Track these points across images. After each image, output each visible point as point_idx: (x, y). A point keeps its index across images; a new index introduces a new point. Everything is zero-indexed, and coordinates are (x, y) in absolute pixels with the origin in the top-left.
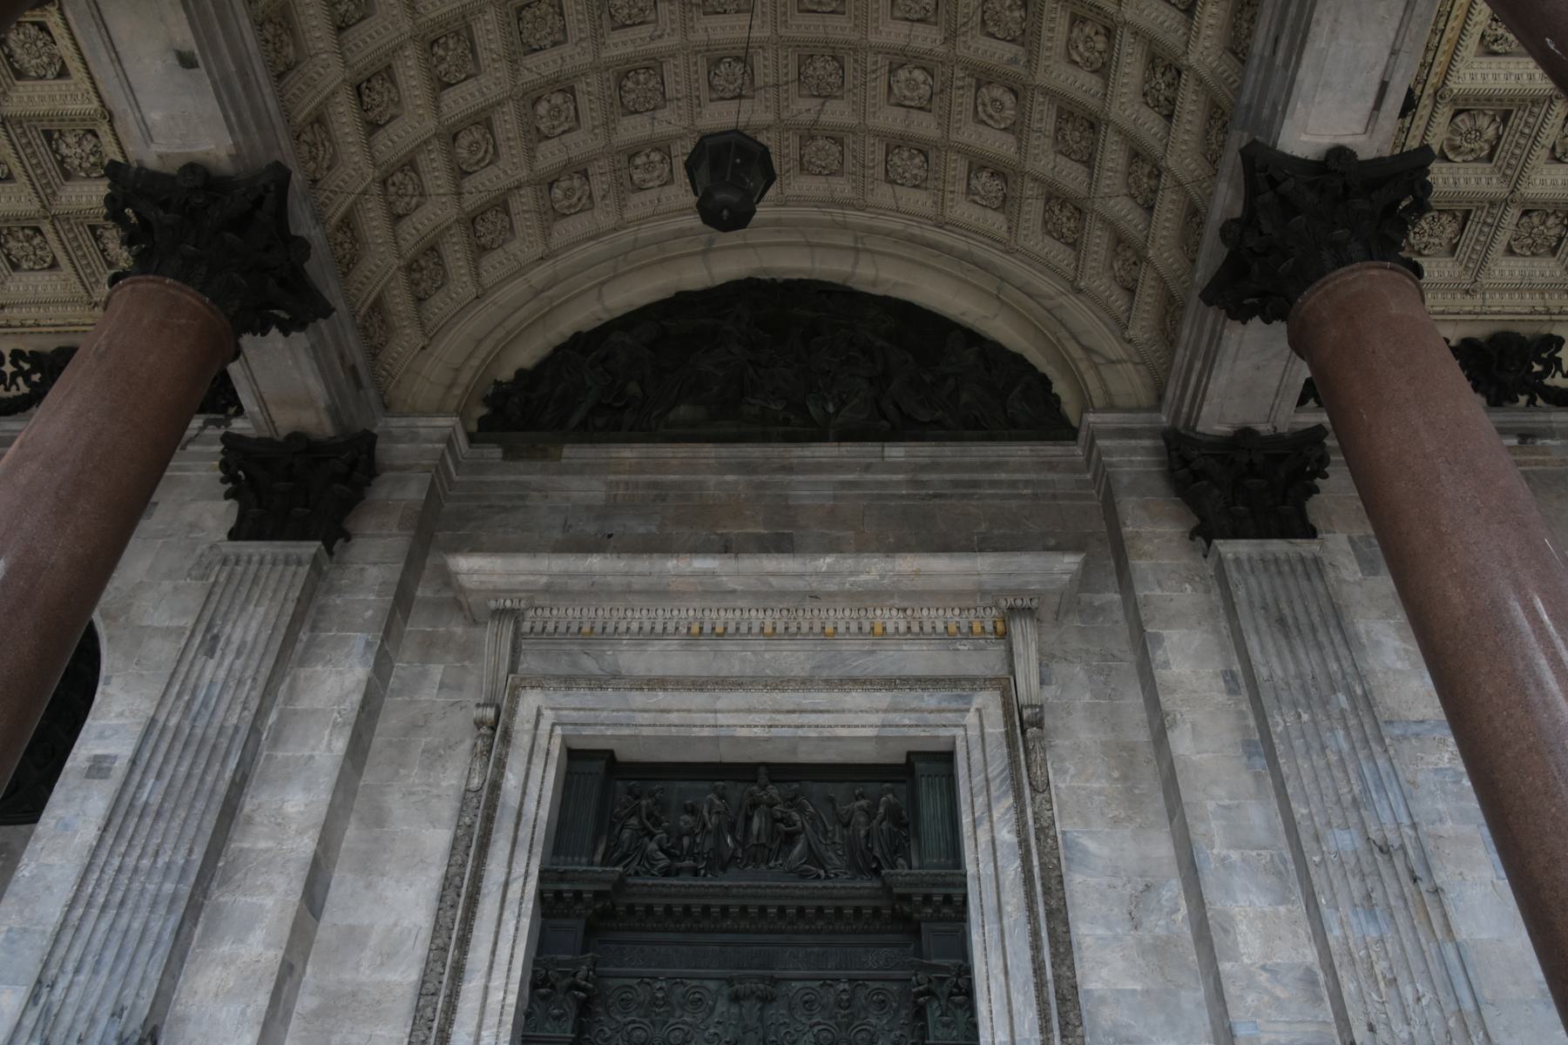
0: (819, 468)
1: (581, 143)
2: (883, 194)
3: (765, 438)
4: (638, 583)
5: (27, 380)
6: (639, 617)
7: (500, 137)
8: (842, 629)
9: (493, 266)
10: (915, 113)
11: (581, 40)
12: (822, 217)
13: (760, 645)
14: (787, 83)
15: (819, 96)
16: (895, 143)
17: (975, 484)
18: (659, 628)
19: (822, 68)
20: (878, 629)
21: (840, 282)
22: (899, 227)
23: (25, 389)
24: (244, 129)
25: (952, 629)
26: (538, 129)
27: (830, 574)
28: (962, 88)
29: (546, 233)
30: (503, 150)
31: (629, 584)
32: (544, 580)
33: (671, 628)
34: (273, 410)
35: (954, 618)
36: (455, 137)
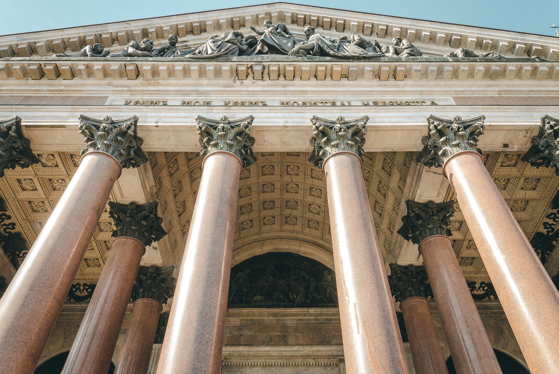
0: (293, 315)
2: (307, 230)
3: (279, 306)
4: (251, 354)
5: (87, 291)
6: (251, 361)
8: (300, 364)
10: (316, 215)
13: (280, 368)
17: (331, 320)
18: (256, 364)
20: (308, 364)
21: (296, 253)
23: (86, 294)
25: (326, 364)
27: (297, 351)
31: (249, 354)
32: (228, 353)
33: (259, 364)
35: (326, 361)
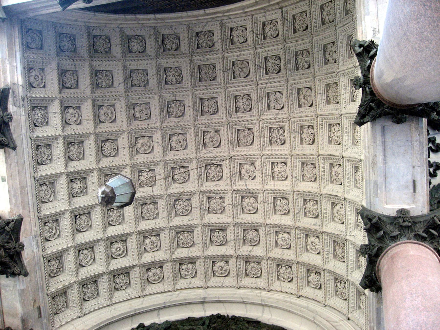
1: (159, 256)
2: (277, 285)
7: (129, 248)
9: (118, 296)
11: (164, 218)
12: (252, 294)
14: (239, 240)
15: (251, 245)
16: (280, 263)
19: (251, 235)
22: (282, 298)
24: (16, 205)
26: (145, 248)
28: (300, 238)
29: (143, 289)
30: (129, 252)
34: (5, 316)
36: (111, 244)
